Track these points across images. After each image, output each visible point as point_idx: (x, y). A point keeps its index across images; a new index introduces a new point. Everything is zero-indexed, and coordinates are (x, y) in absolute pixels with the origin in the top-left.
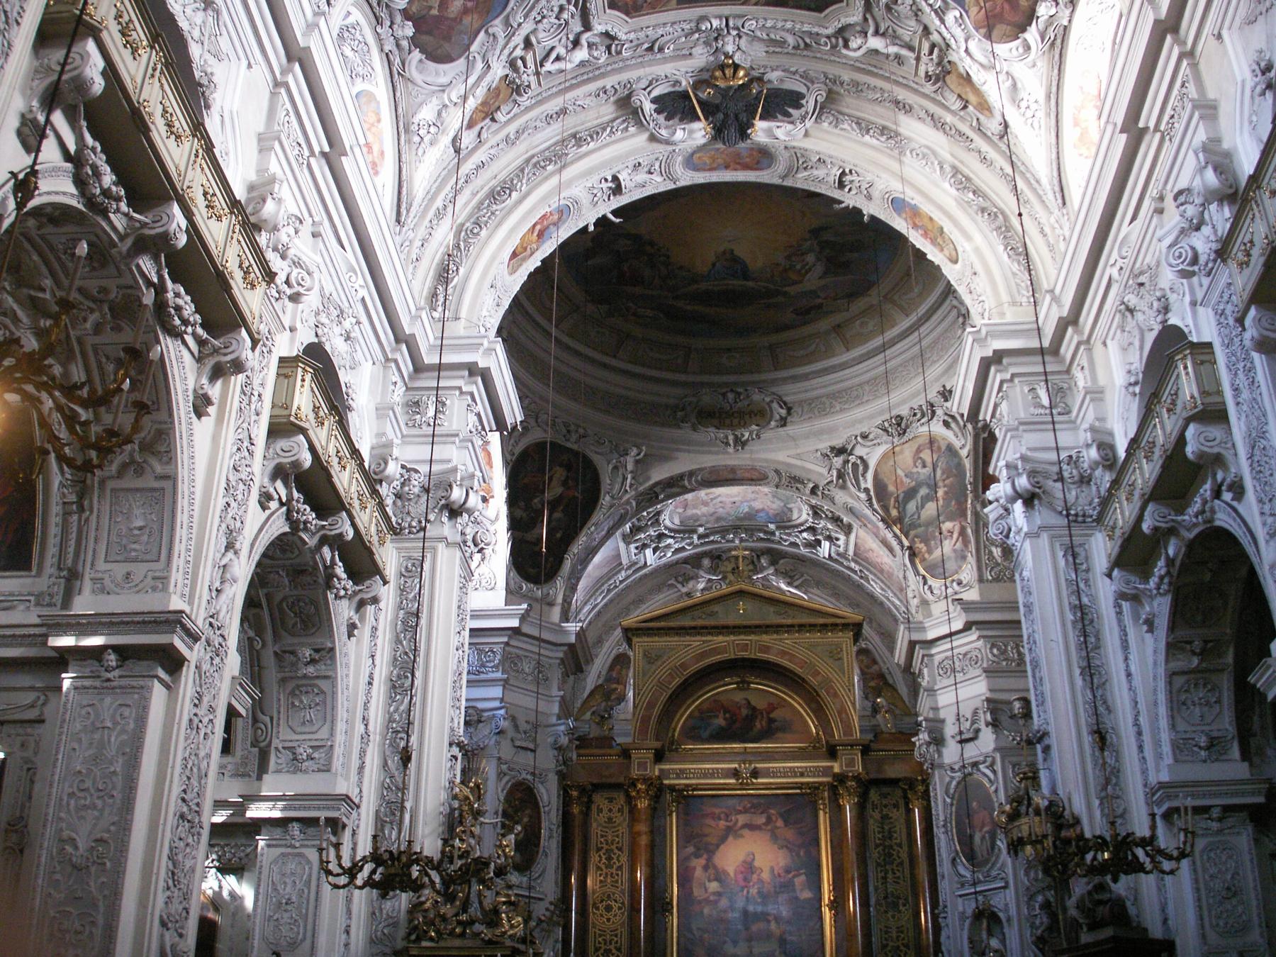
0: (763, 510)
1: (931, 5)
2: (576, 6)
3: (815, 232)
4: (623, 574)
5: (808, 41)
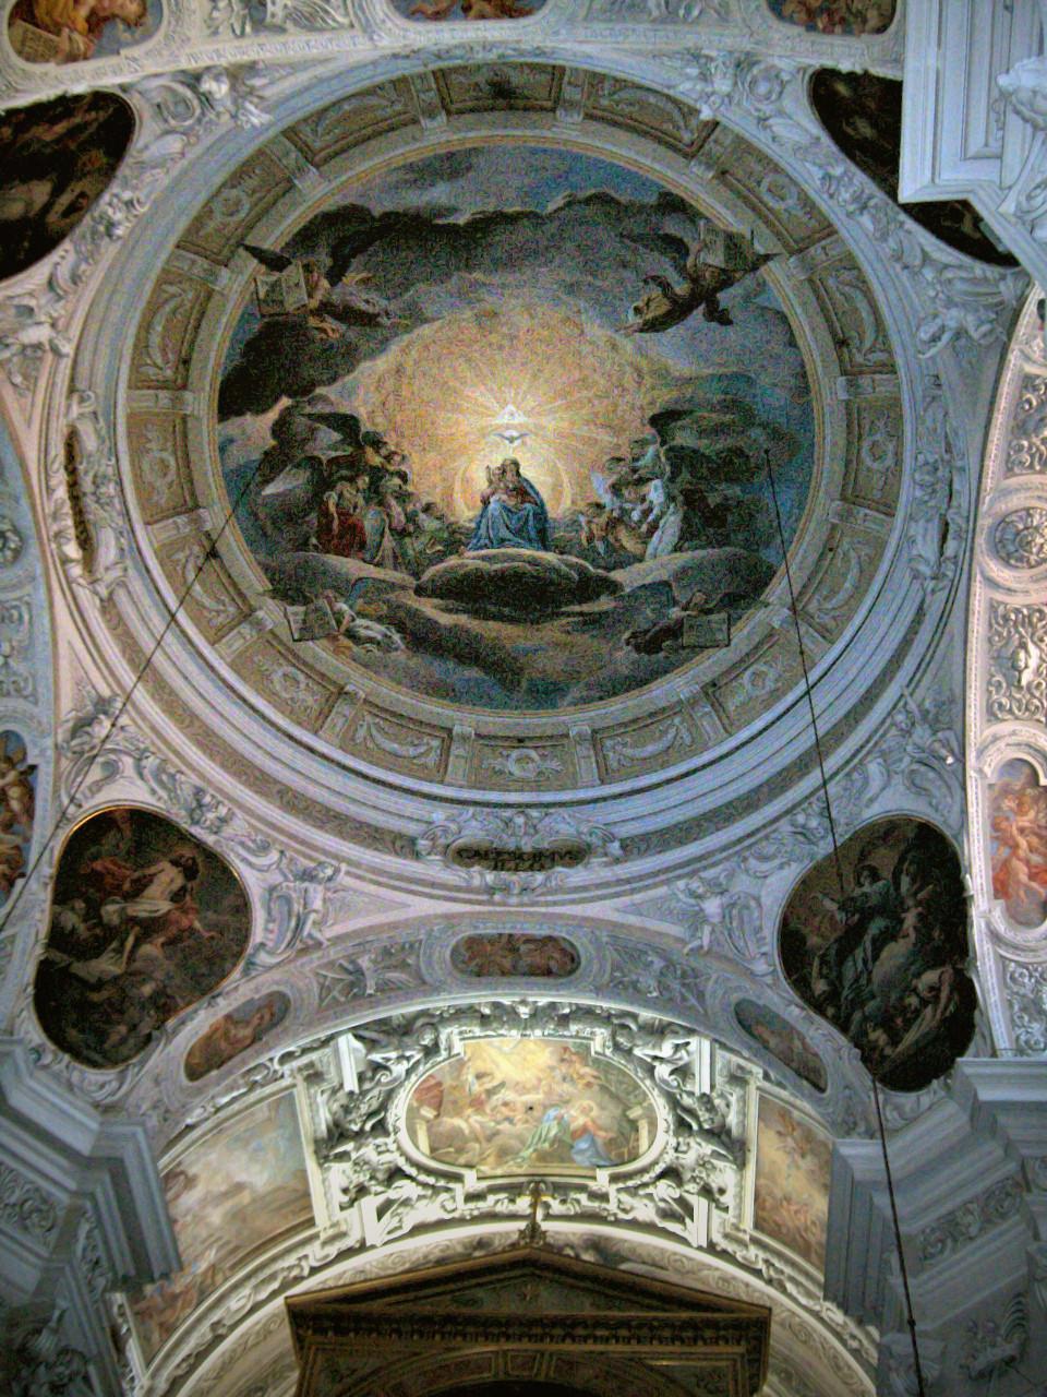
0: (584, 1130)
3: (663, 421)
4: (315, 1253)
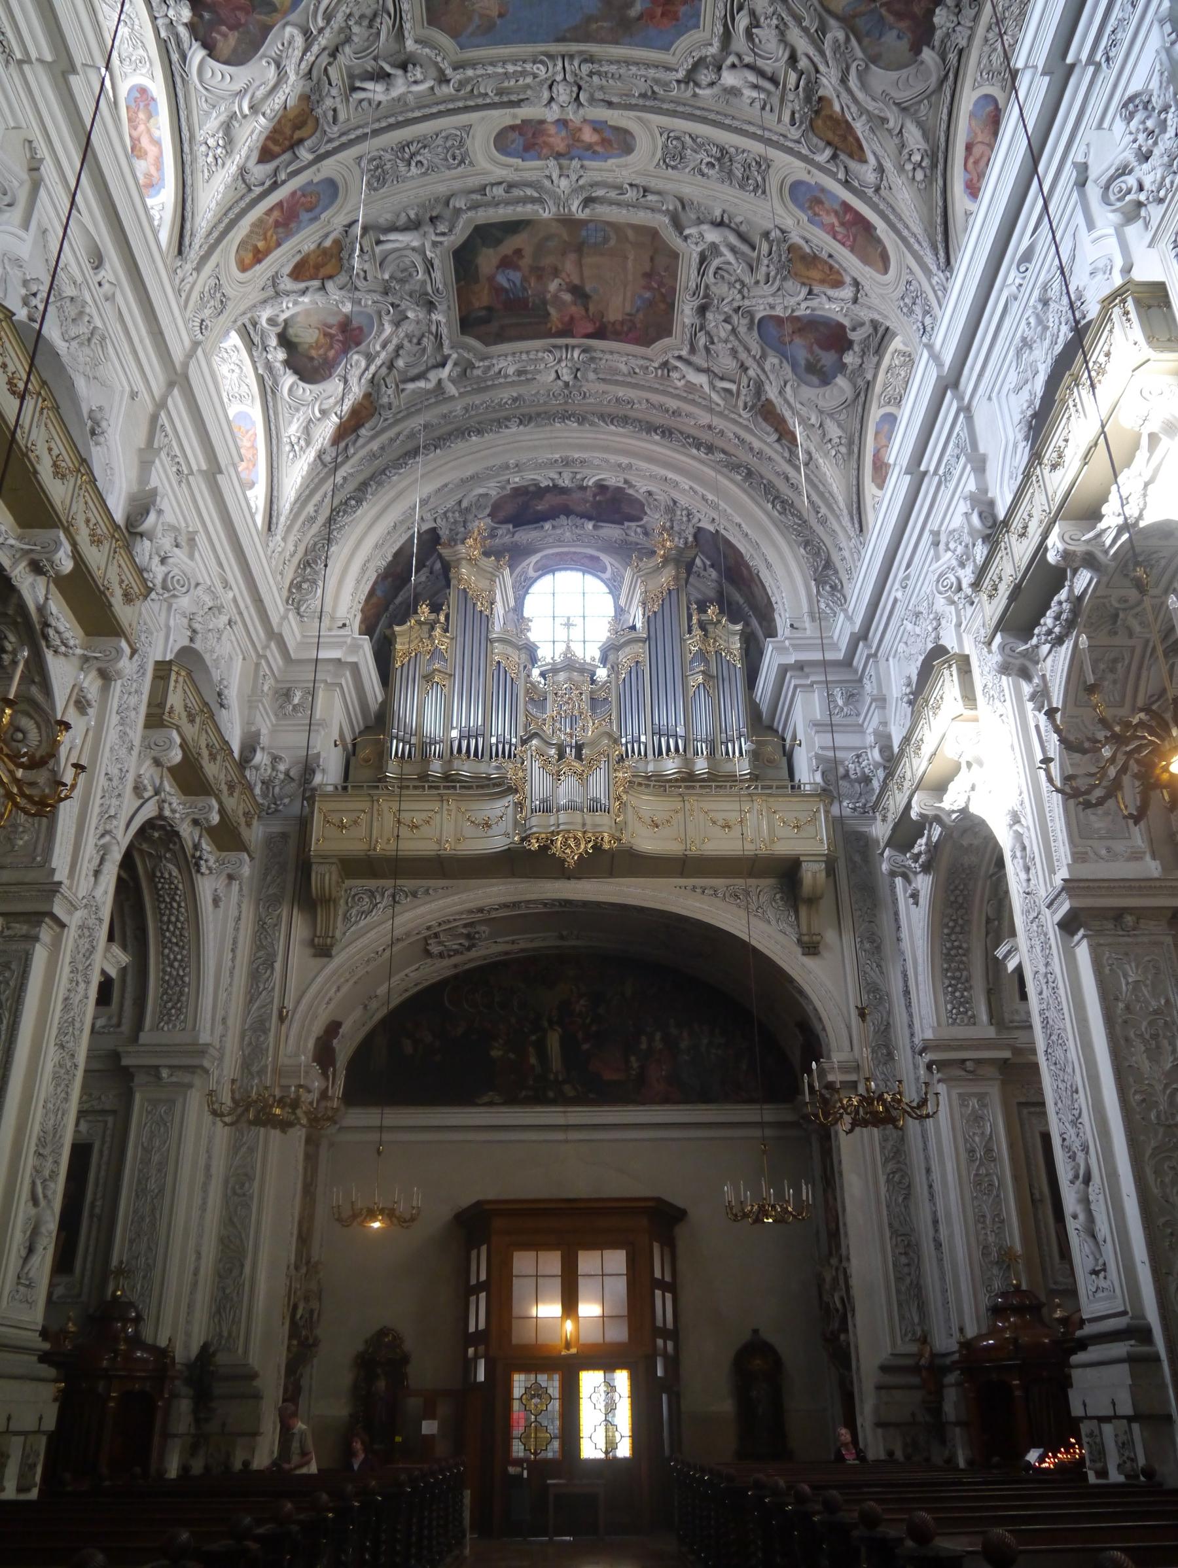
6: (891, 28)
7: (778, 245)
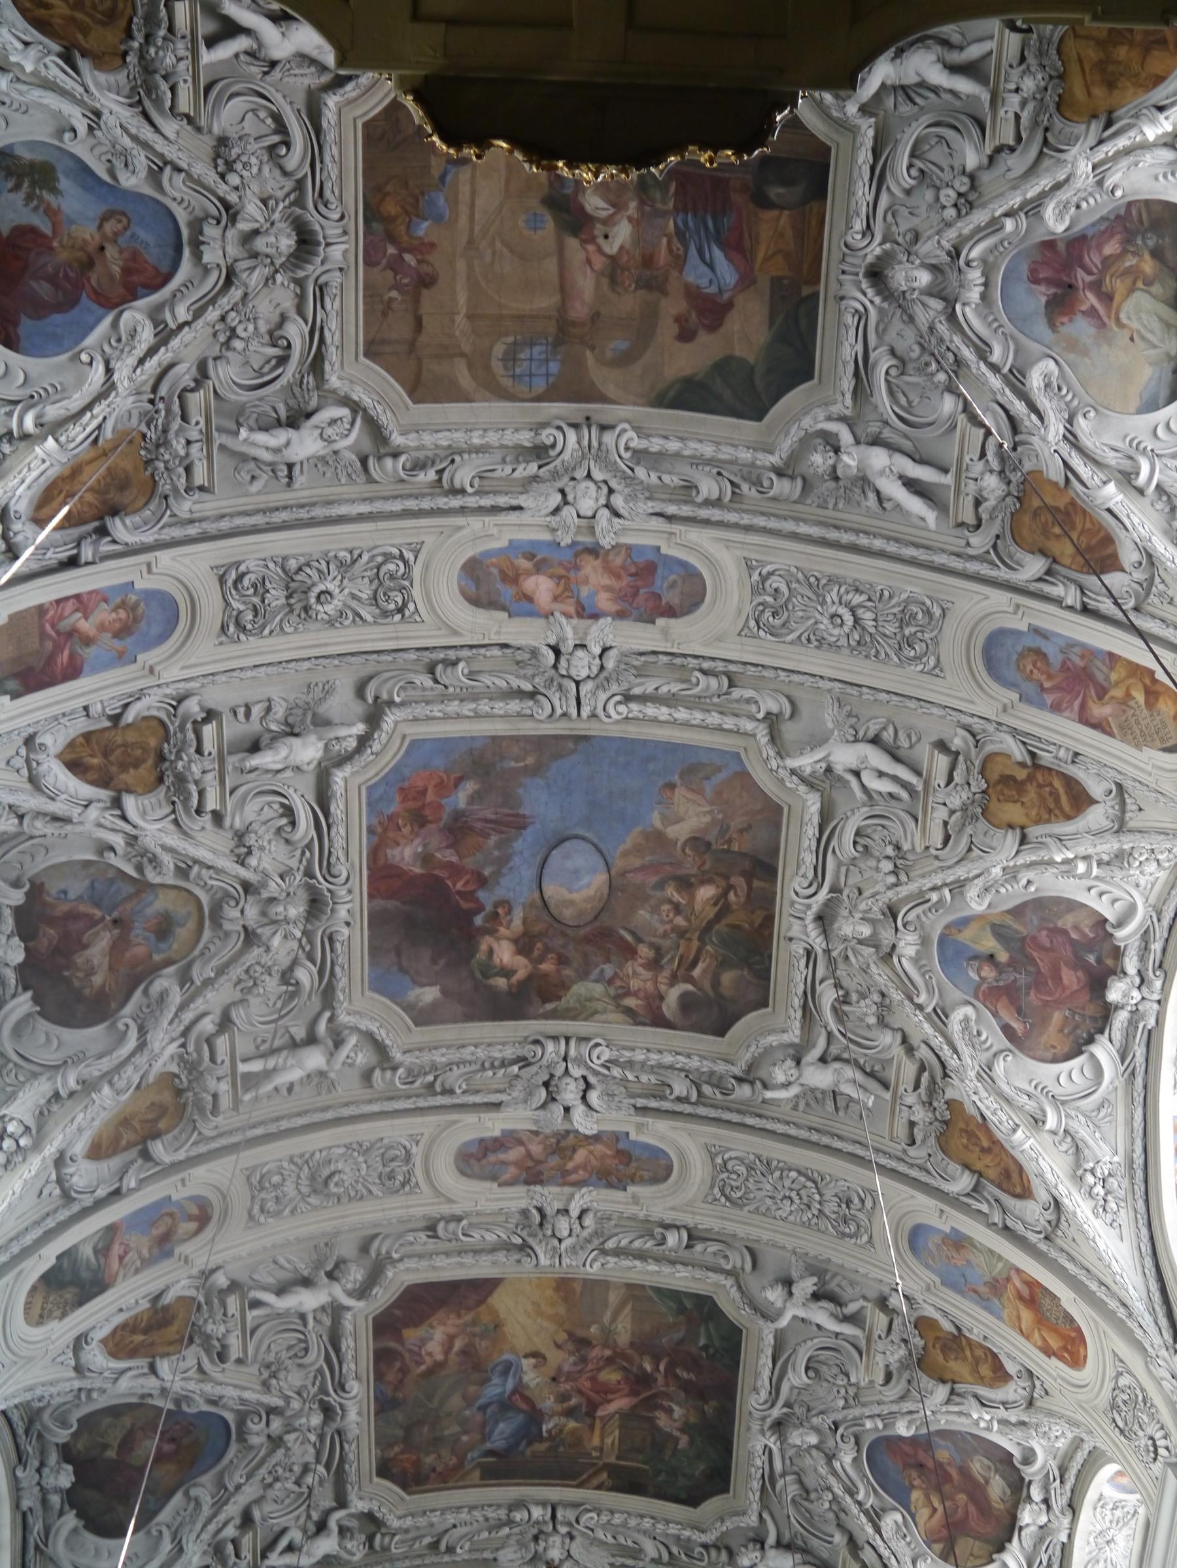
1: (859, 1503)
2: (328, 1467)
5: (675, 1550)
6: (80, 898)
7: (175, 490)
